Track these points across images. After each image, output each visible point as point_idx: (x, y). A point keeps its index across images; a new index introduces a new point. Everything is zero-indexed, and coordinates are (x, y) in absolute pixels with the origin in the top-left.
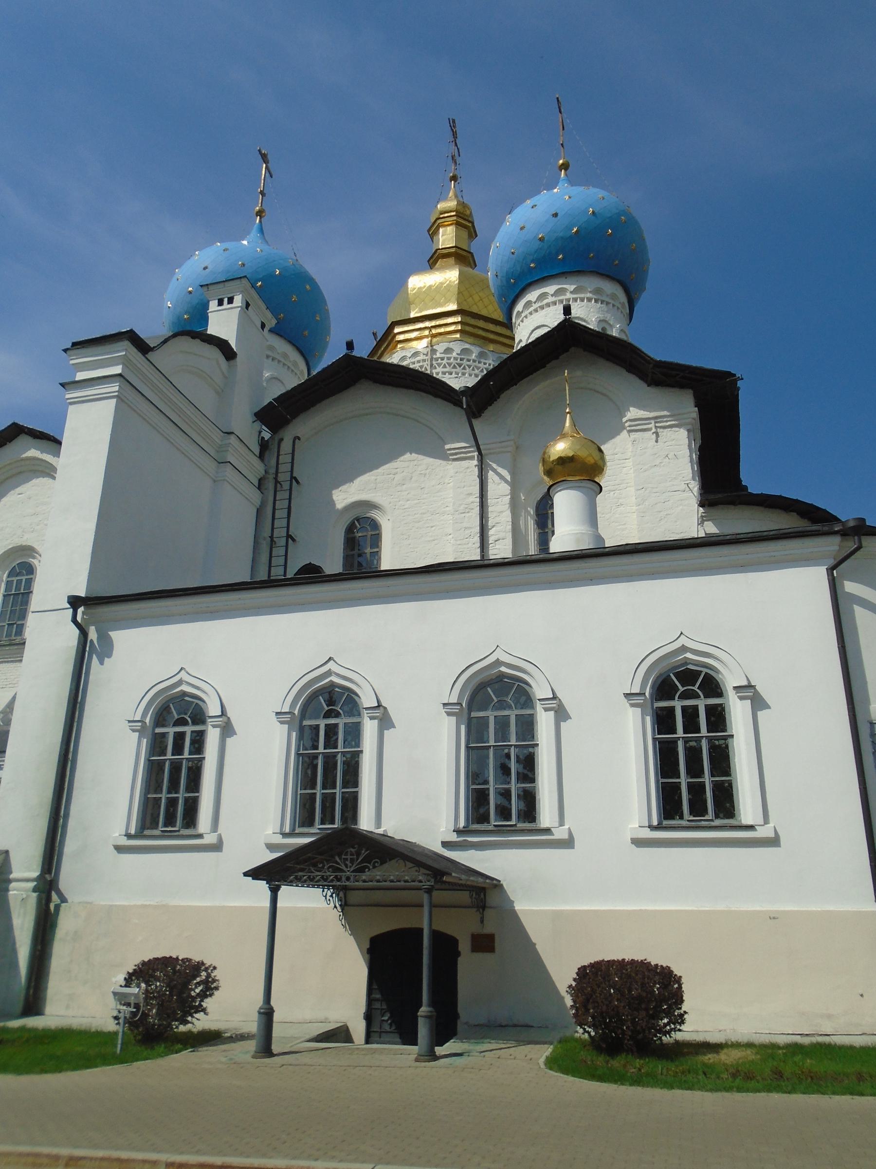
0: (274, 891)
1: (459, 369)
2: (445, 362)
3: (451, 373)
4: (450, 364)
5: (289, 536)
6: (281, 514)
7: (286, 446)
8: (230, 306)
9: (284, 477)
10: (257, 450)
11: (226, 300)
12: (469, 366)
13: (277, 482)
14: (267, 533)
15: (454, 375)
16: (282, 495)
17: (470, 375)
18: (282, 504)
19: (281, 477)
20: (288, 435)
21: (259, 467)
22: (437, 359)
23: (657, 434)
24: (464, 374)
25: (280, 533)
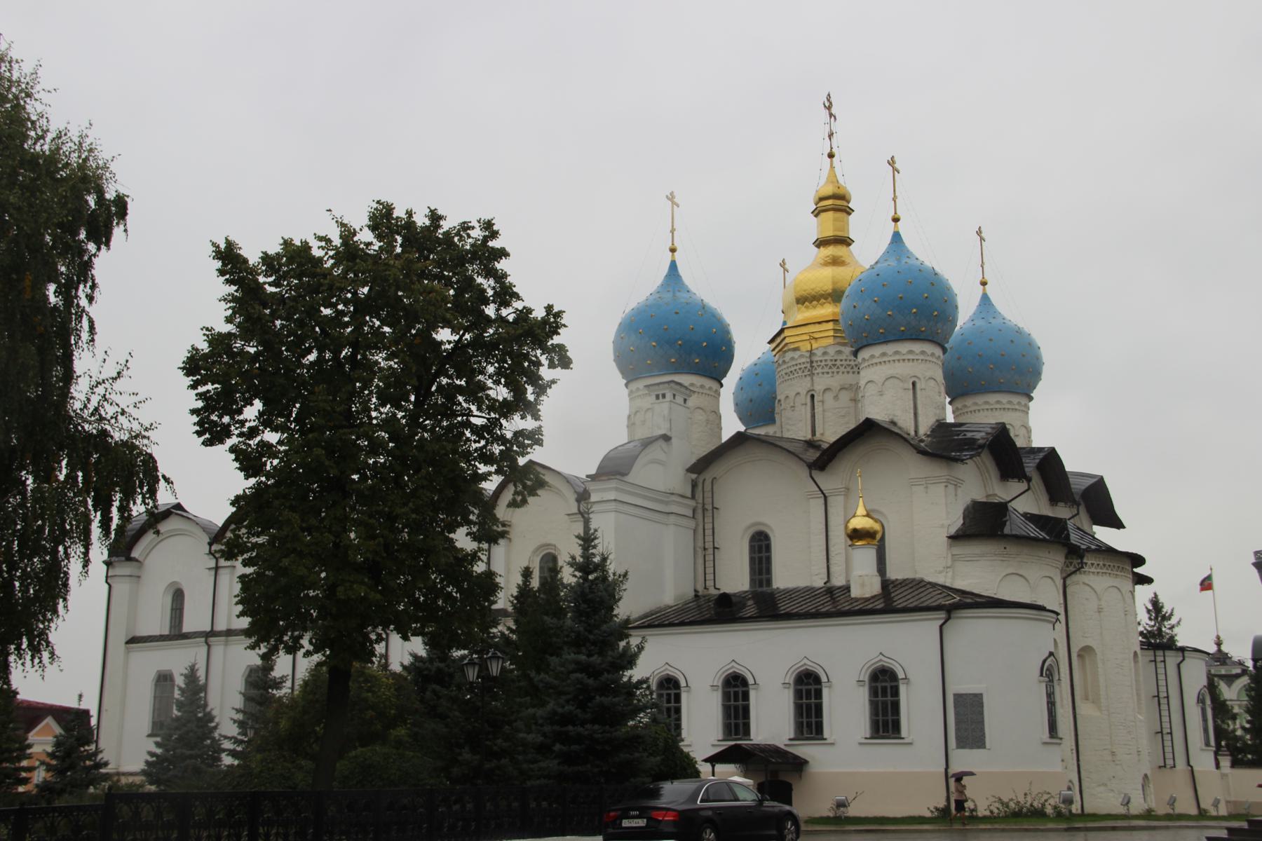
0: (713, 767)
1: (835, 370)
2: (823, 363)
3: (828, 373)
4: (826, 365)
5: (714, 548)
6: (709, 532)
7: (708, 483)
8: (664, 400)
9: (709, 507)
10: (689, 494)
11: (661, 396)
12: (842, 365)
13: (704, 510)
14: (700, 544)
15: (830, 375)
16: (708, 520)
17: (843, 373)
18: (709, 526)
19: (706, 507)
20: (708, 475)
21: (692, 503)
22: (817, 362)
23: (927, 487)
24: (838, 372)
25: (709, 545)
